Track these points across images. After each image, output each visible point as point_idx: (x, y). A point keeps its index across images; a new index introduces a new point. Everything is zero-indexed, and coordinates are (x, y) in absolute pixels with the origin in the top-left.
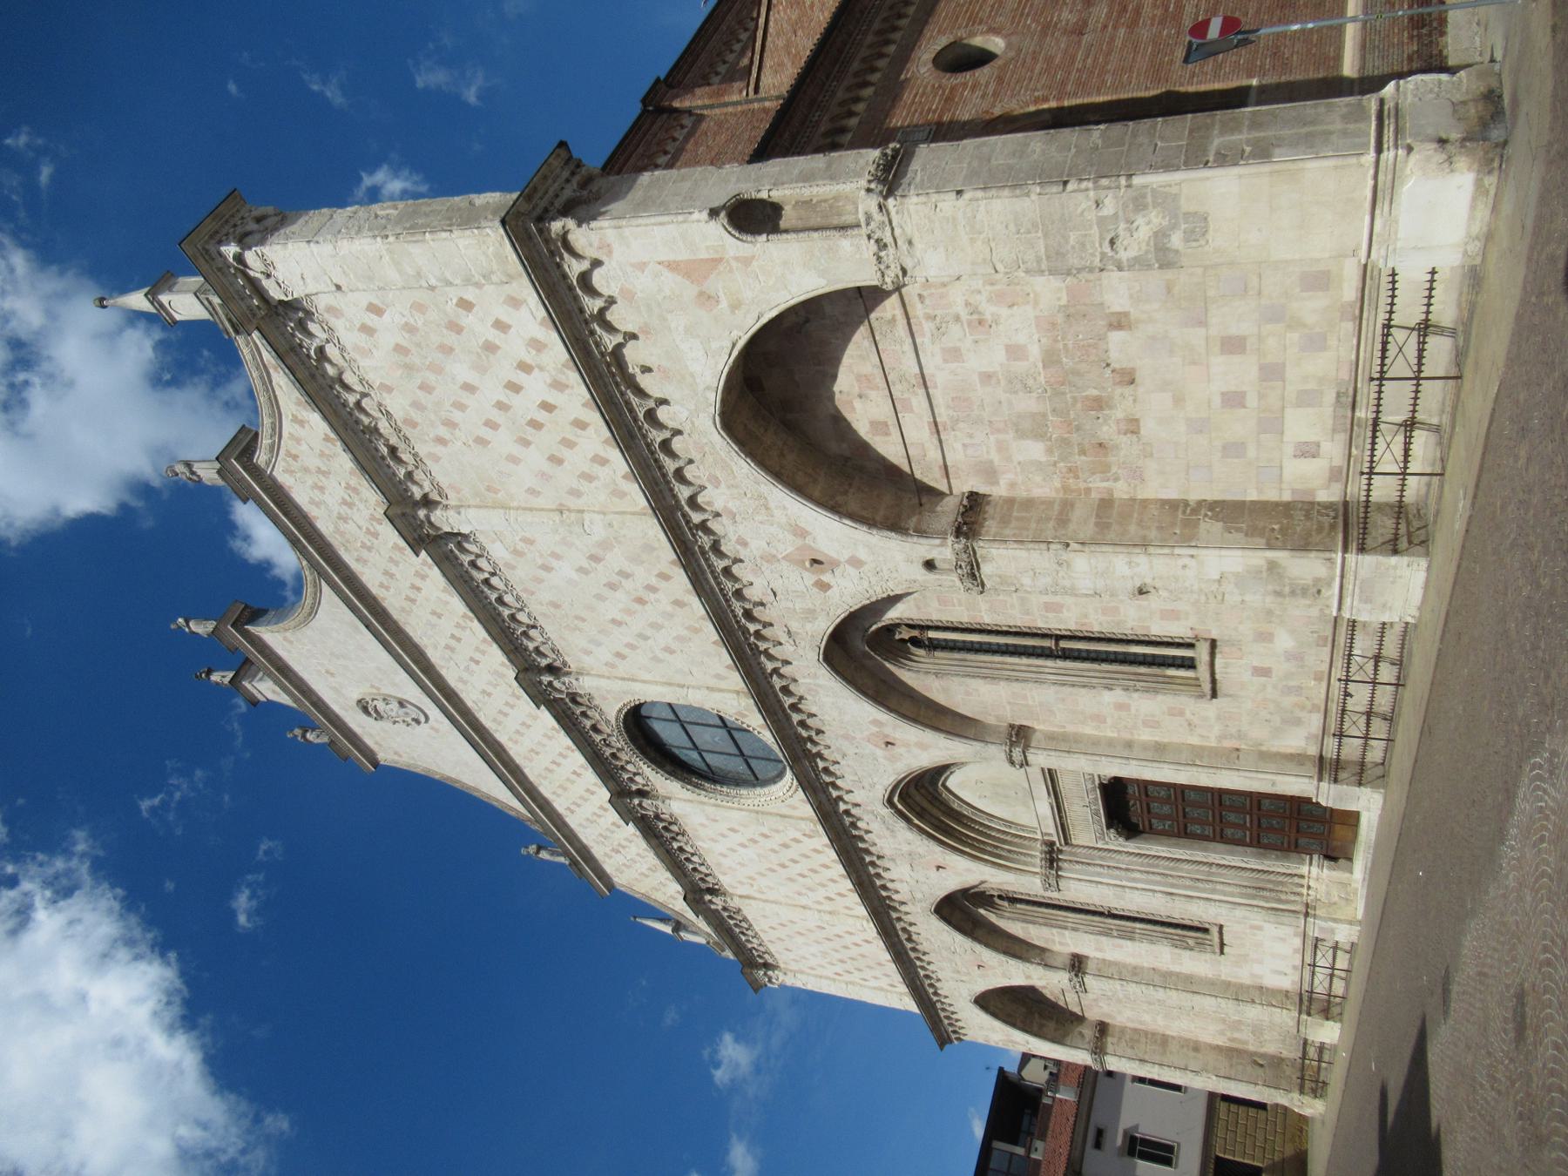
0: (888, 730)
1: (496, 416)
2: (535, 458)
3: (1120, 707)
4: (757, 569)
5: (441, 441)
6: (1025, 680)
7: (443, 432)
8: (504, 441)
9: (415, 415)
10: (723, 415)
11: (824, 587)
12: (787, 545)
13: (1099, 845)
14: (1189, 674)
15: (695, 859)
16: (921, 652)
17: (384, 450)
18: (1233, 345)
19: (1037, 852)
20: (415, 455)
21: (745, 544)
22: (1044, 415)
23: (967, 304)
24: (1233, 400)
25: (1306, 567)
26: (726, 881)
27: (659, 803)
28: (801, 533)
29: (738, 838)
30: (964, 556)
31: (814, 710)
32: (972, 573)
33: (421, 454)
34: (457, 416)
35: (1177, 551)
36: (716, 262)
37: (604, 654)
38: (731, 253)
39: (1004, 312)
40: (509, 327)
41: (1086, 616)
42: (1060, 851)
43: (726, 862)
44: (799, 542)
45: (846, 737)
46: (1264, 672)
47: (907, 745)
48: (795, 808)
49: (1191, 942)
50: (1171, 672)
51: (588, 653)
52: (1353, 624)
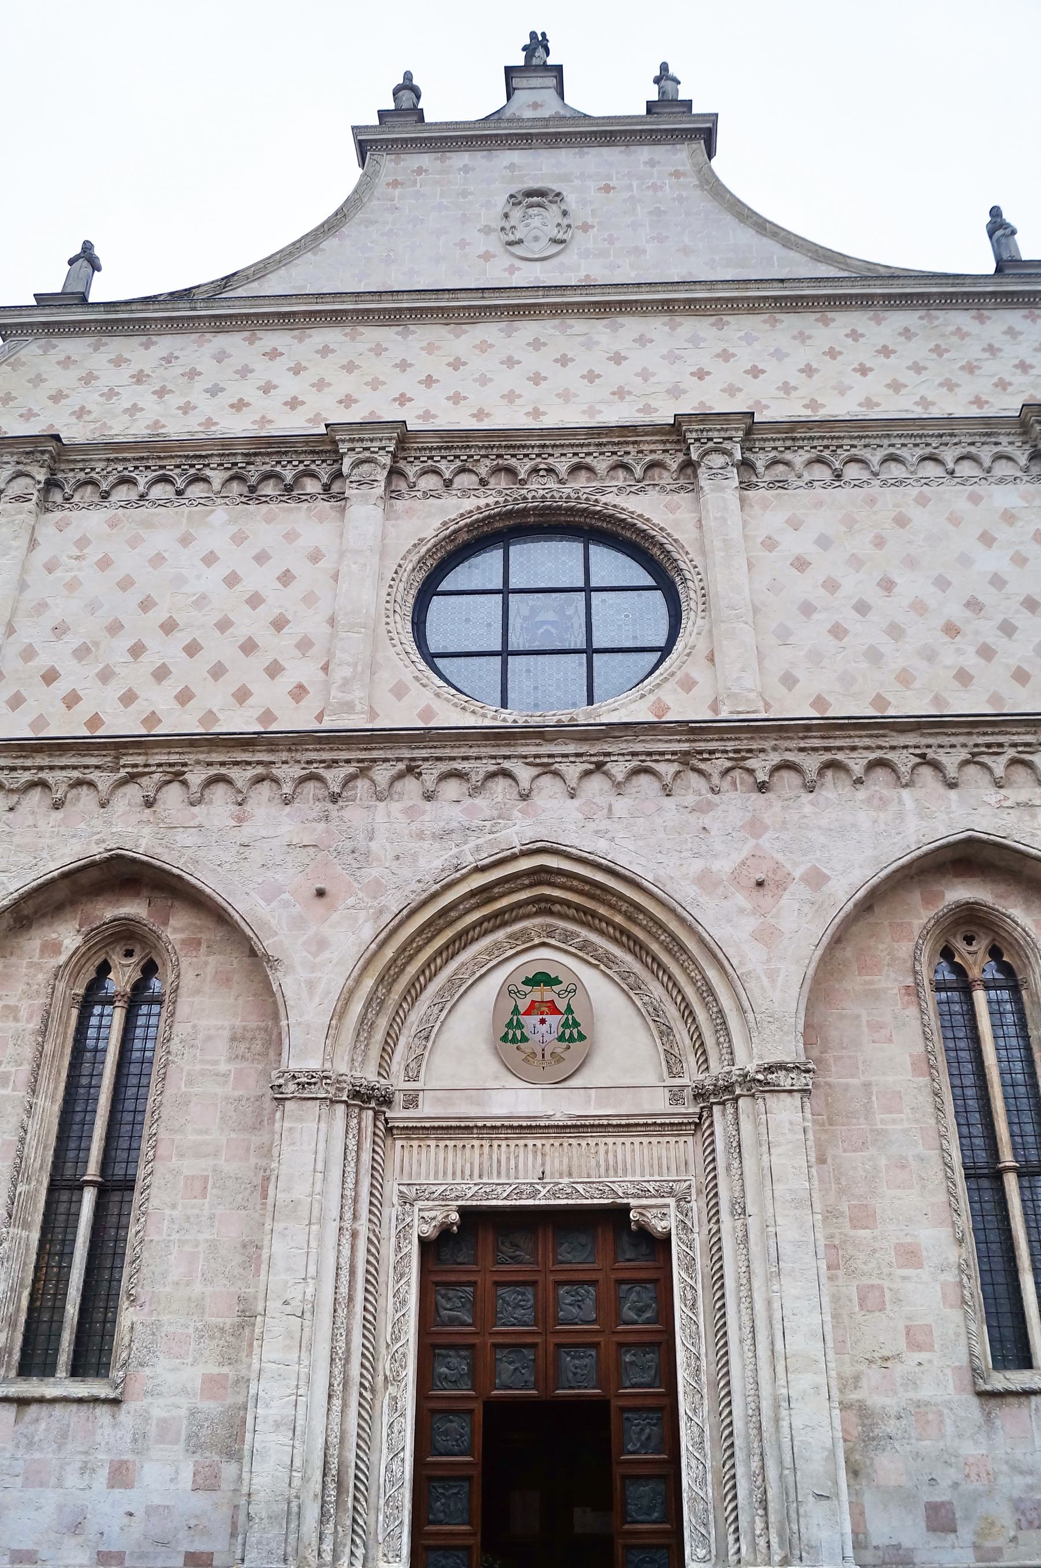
3: (910, 1255)
42: (376, 1113)
45: (755, 827)
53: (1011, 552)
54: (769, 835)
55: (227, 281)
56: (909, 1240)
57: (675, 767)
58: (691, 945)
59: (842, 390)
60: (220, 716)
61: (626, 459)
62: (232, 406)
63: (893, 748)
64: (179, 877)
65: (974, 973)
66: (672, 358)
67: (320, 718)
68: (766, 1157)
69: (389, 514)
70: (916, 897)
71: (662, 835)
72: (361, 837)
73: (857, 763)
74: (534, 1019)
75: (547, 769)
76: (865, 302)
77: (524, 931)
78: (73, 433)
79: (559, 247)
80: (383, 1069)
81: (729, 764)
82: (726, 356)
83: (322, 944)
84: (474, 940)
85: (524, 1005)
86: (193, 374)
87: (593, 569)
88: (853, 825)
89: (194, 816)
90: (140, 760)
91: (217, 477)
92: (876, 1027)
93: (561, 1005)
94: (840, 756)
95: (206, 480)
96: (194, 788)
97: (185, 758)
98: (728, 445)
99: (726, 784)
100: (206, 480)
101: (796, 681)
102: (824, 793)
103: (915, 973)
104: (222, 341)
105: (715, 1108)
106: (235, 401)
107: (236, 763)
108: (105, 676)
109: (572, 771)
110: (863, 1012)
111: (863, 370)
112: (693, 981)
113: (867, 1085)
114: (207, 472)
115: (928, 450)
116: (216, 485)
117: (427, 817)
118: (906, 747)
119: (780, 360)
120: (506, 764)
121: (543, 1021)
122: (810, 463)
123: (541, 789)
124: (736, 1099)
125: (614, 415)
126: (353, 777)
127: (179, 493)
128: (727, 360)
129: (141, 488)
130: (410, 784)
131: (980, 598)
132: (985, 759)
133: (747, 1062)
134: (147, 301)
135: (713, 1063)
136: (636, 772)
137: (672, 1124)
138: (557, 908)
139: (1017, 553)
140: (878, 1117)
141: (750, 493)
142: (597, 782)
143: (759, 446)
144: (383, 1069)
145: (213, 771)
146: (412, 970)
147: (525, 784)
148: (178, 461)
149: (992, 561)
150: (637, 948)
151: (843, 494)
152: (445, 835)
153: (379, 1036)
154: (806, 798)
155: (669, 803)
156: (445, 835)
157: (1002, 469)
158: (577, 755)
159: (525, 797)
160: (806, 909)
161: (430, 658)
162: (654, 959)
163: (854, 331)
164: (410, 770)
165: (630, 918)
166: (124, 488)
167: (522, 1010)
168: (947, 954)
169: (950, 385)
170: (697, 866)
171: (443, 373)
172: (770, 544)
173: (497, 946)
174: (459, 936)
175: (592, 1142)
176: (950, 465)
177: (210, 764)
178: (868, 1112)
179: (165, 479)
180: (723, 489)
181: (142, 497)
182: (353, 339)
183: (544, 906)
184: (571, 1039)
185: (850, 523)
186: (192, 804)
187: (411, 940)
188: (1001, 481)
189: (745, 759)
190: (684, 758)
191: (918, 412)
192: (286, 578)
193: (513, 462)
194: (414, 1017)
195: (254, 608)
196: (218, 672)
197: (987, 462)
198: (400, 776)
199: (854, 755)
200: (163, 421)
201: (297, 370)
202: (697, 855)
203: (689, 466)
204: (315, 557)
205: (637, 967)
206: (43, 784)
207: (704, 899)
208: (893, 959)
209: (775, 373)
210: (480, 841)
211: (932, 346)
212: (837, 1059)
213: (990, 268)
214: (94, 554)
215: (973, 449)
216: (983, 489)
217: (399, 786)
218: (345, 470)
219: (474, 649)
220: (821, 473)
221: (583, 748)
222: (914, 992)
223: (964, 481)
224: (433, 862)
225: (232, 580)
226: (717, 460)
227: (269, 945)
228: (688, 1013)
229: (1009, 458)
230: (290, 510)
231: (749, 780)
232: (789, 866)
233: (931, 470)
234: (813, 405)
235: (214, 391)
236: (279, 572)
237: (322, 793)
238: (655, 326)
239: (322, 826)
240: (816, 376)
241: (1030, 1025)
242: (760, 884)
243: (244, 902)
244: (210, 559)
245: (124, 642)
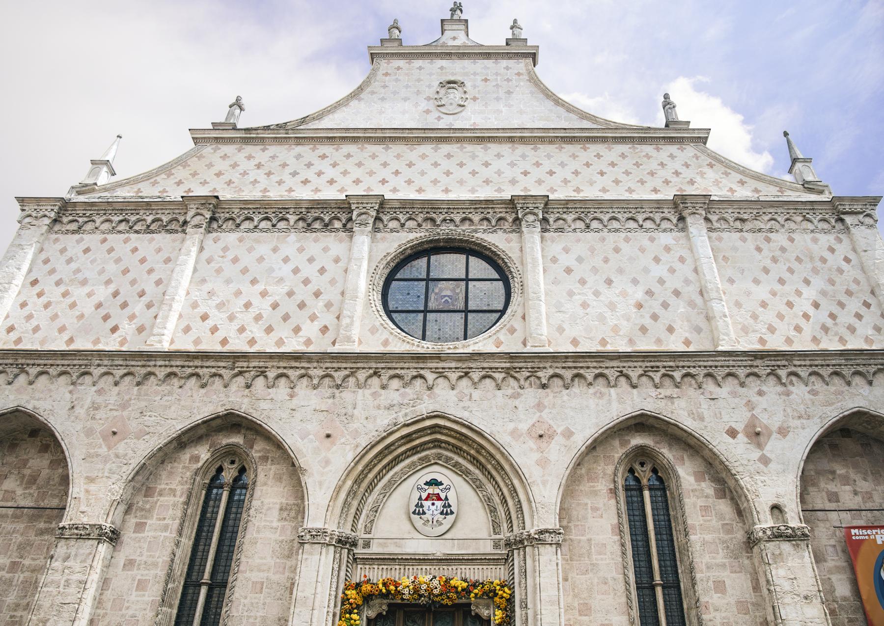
0: (559, 439)
10: (865, 413)
11: (732, 433)
17: (745, 216)
30: (799, 533)
44: (774, 428)
45: (540, 406)
53: (668, 267)
54: (547, 411)
55: (304, 120)
56: (607, 622)
57: (503, 375)
58: (507, 467)
59: (592, 183)
60: (285, 340)
61: (488, 216)
62: (302, 182)
63: (607, 368)
64: (260, 425)
65: (644, 482)
66: (512, 164)
67: (334, 343)
68: (538, 579)
69: (373, 240)
70: (616, 443)
71: (495, 410)
72: (350, 407)
73: (589, 375)
74: (429, 503)
75: (441, 375)
76: (604, 140)
77: (426, 457)
78: (226, 195)
79: (461, 109)
81: (528, 374)
82: (538, 164)
83: (327, 462)
84: (402, 460)
85: (424, 496)
86: (284, 165)
87: (470, 269)
88: (587, 406)
89: (269, 394)
90: (245, 364)
91: (292, 218)
92: (595, 509)
93: (443, 496)
94: (582, 371)
95: (287, 220)
96: (270, 380)
97: (267, 364)
98: (536, 211)
99: (527, 384)
100: (287, 220)
101: (564, 330)
102: (574, 389)
103: (615, 482)
104: (299, 149)
105: (516, 552)
106: (303, 179)
107: (292, 368)
108: (231, 318)
109: (454, 376)
110: (589, 502)
111: (602, 173)
112: (507, 486)
113: (589, 540)
114: (288, 216)
115: (630, 215)
116: (292, 222)
117: (382, 398)
118: (613, 367)
119: (563, 167)
120: (422, 372)
121: (433, 504)
122: (575, 220)
123: (438, 385)
124: (525, 547)
125: (483, 194)
126: (348, 376)
127: (274, 226)
128: (538, 167)
129: (256, 223)
130: (375, 381)
131: (653, 290)
132: (651, 374)
133: (532, 530)
134: (267, 128)
135: (515, 528)
136: (484, 377)
137: (494, 559)
138: (443, 445)
139: (671, 267)
140: (594, 557)
141: (546, 234)
142: (465, 382)
143: (549, 213)
145: (280, 371)
146: (371, 476)
147: (430, 382)
148: (274, 210)
149: (659, 271)
150: (482, 467)
151: (590, 235)
152: (390, 407)
153: (353, 510)
154: (565, 392)
155: (499, 393)
156: (390, 407)
157: (665, 225)
158: (456, 368)
159: (430, 388)
160: (563, 449)
161: (389, 313)
162: (489, 473)
163: (598, 154)
164: (375, 373)
165: (478, 452)
166: (247, 222)
167: (424, 498)
168: (631, 471)
169: (642, 182)
170: (511, 426)
171: (403, 168)
172: (554, 260)
173: (413, 464)
174: (395, 459)
175: (454, 568)
176: (641, 223)
177: (278, 368)
178: (589, 554)
179: (267, 219)
180: (533, 232)
181: (256, 227)
182: (362, 150)
183: (437, 444)
184: (447, 514)
185: (592, 250)
186: (268, 387)
188: (665, 231)
189: (536, 372)
190: (508, 371)
191: (626, 196)
192: (322, 271)
193: (434, 215)
194: (371, 500)
195: (306, 285)
196: (286, 318)
197: (658, 222)
198: (370, 376)
199: (588, 371)
200: (269, 188)
201: (334, 165)
202: (511, 421)
203: (517, 220)
204: (337, 260)
205: (481, 476)
206: (197, 375)
207: (513, 443)
208: (605, 474)
209: (561, 174)
210: (407, 411)
211: (634, 162)
212: (576, 526)
213: (662, 125)
214: (230, 255)
215: (651, 215)
216: (655, 234)
217: (369, 381)
218: (354, 218)
219: (411, 309)
220: (580, 225)
221: (459, 365)
222: (614, 492)
223: (647, 230)
224: (384, 421)
225: (296, 271)
226: (531, 218)
227: (302, 462)
228: (504, 501)
229: (668, 220)
230: (326, 236)
231: (538, 382)
232: (555, 428)
233: (632, 224)
234: (578, 190)
235: (294, 174)
236: (319, 267)
237: (331, 384)
238: (505, 148)
239: (331, 400)
240: (580, 176)
241: (670, 509)
242: (541, 436)
243: (291, 439)
244: (286, 260)
245: (241, 301)
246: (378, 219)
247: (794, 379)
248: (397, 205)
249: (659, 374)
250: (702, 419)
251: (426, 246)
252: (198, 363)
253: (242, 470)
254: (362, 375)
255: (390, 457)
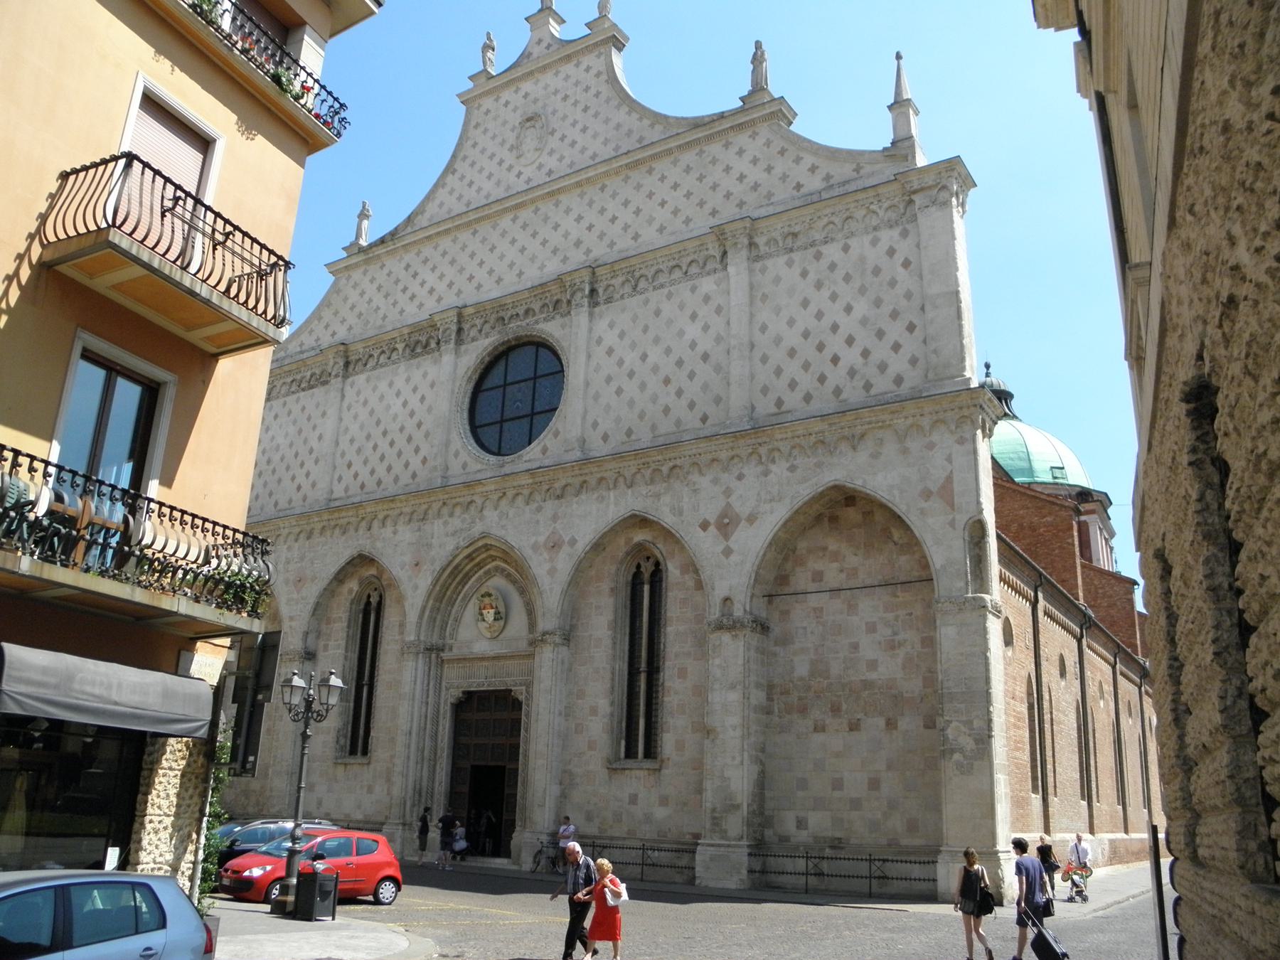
0: (566, 548)
1: (826, 322)
2: (792, 338)
3: (594, 711)
4: (715, 481)
5: (804, 274)
6: (614, 648)
7: (812, 277)
8: (805, 319)
9: (824, 263)
11: (705, 526)
12: (742, 509)
13: (444, 684)
14: (622, 755)
15: (383, 359)
16: (630, 578)
17: (797, 229)
18: (874, 784)
19: (435, 640)
20: (791, 250)
21: (740, 477)
22: (828, 678)
23: (905, 641)
24: (838, 784)
25: (735, 825)
26: (360, 379)
27: (452, 345)
28: (751, 519)
29: (414, 402)
31: (583, 497)
32: (720, 627)
33: (793, 255)
34: (826, 293)
35: (746, 754)
36: (952, 505)
37: (611, 338)
38: (958, 517)
39: (900, 661)
40: (896, 352)
41: (676, 693)
43: (383, 386)
45: (555, 518)
46: (633, 799)
47: (551, 560)
48: (456, 455)
49: (342, 741)
50: (623, 743)
51: (611, 326)
52: (694, 852)
80: (442, 636)
130: (445, 511)
144: (442, 636)
170: (533, 540)
173: (480, 578)
187: (446, 581)
222: (613, 590)
224: (450, 545)
246: (460, 330)
247: (776, 454)
248: (470, 310)
249: (649, 471)
250: (681, 513)
251: (501, 349)
252: (336, 515)
253: (381, 596)
254: (436, 506)
255: (461, 576)
